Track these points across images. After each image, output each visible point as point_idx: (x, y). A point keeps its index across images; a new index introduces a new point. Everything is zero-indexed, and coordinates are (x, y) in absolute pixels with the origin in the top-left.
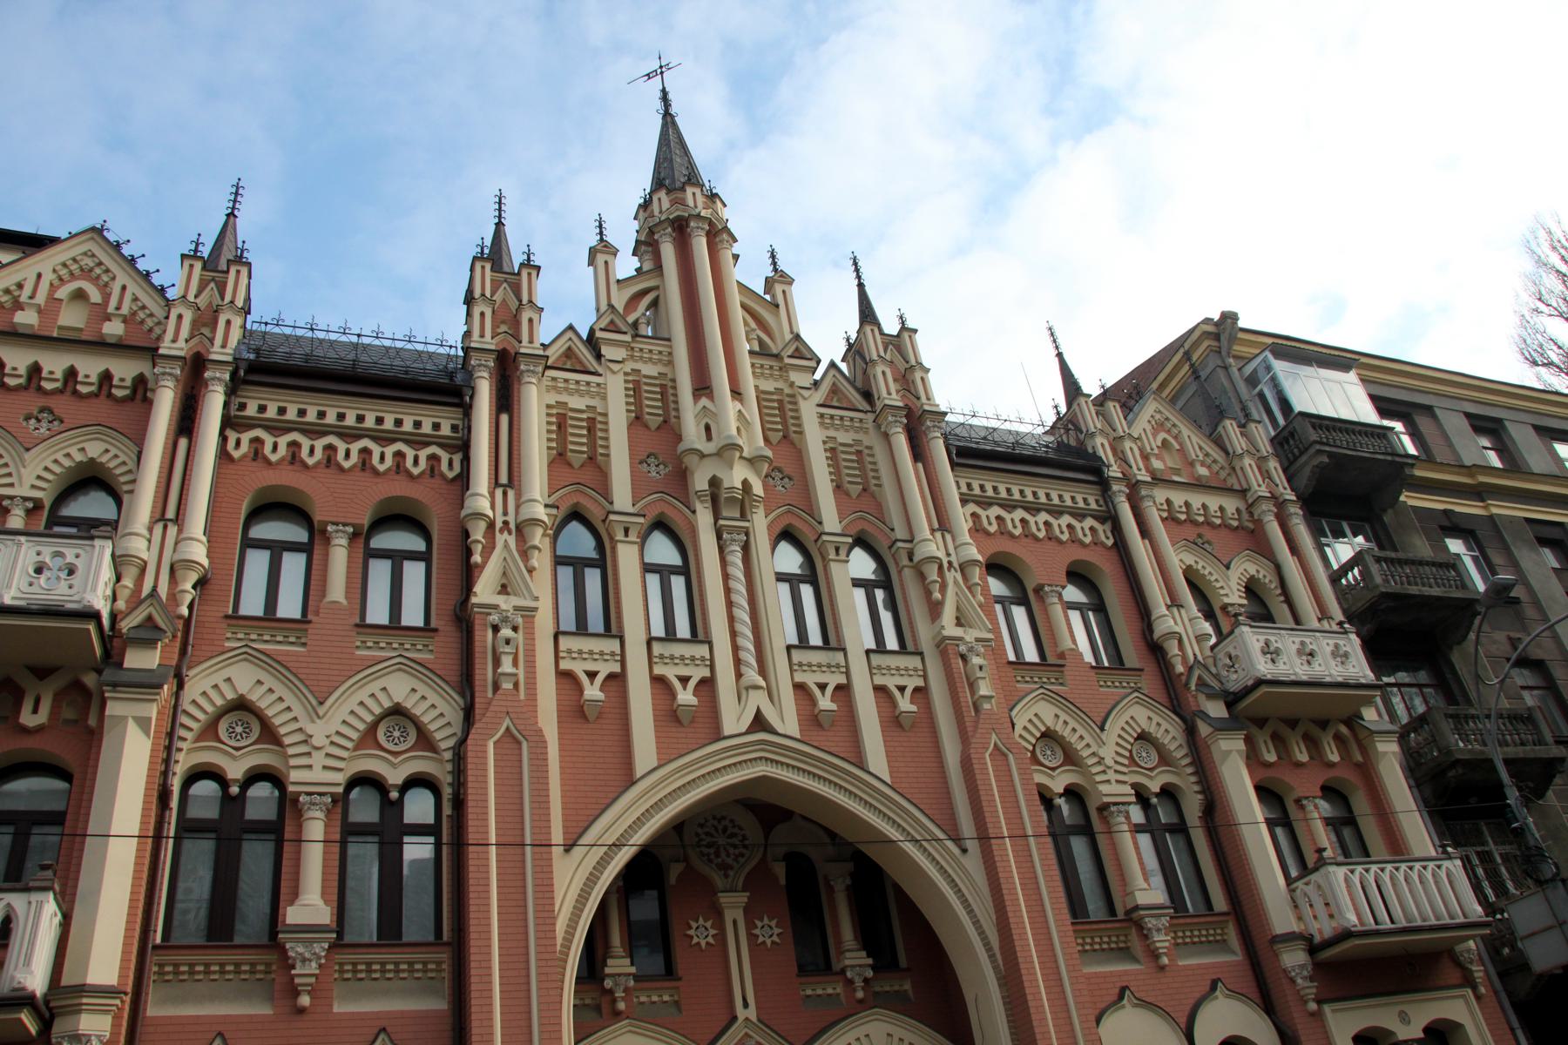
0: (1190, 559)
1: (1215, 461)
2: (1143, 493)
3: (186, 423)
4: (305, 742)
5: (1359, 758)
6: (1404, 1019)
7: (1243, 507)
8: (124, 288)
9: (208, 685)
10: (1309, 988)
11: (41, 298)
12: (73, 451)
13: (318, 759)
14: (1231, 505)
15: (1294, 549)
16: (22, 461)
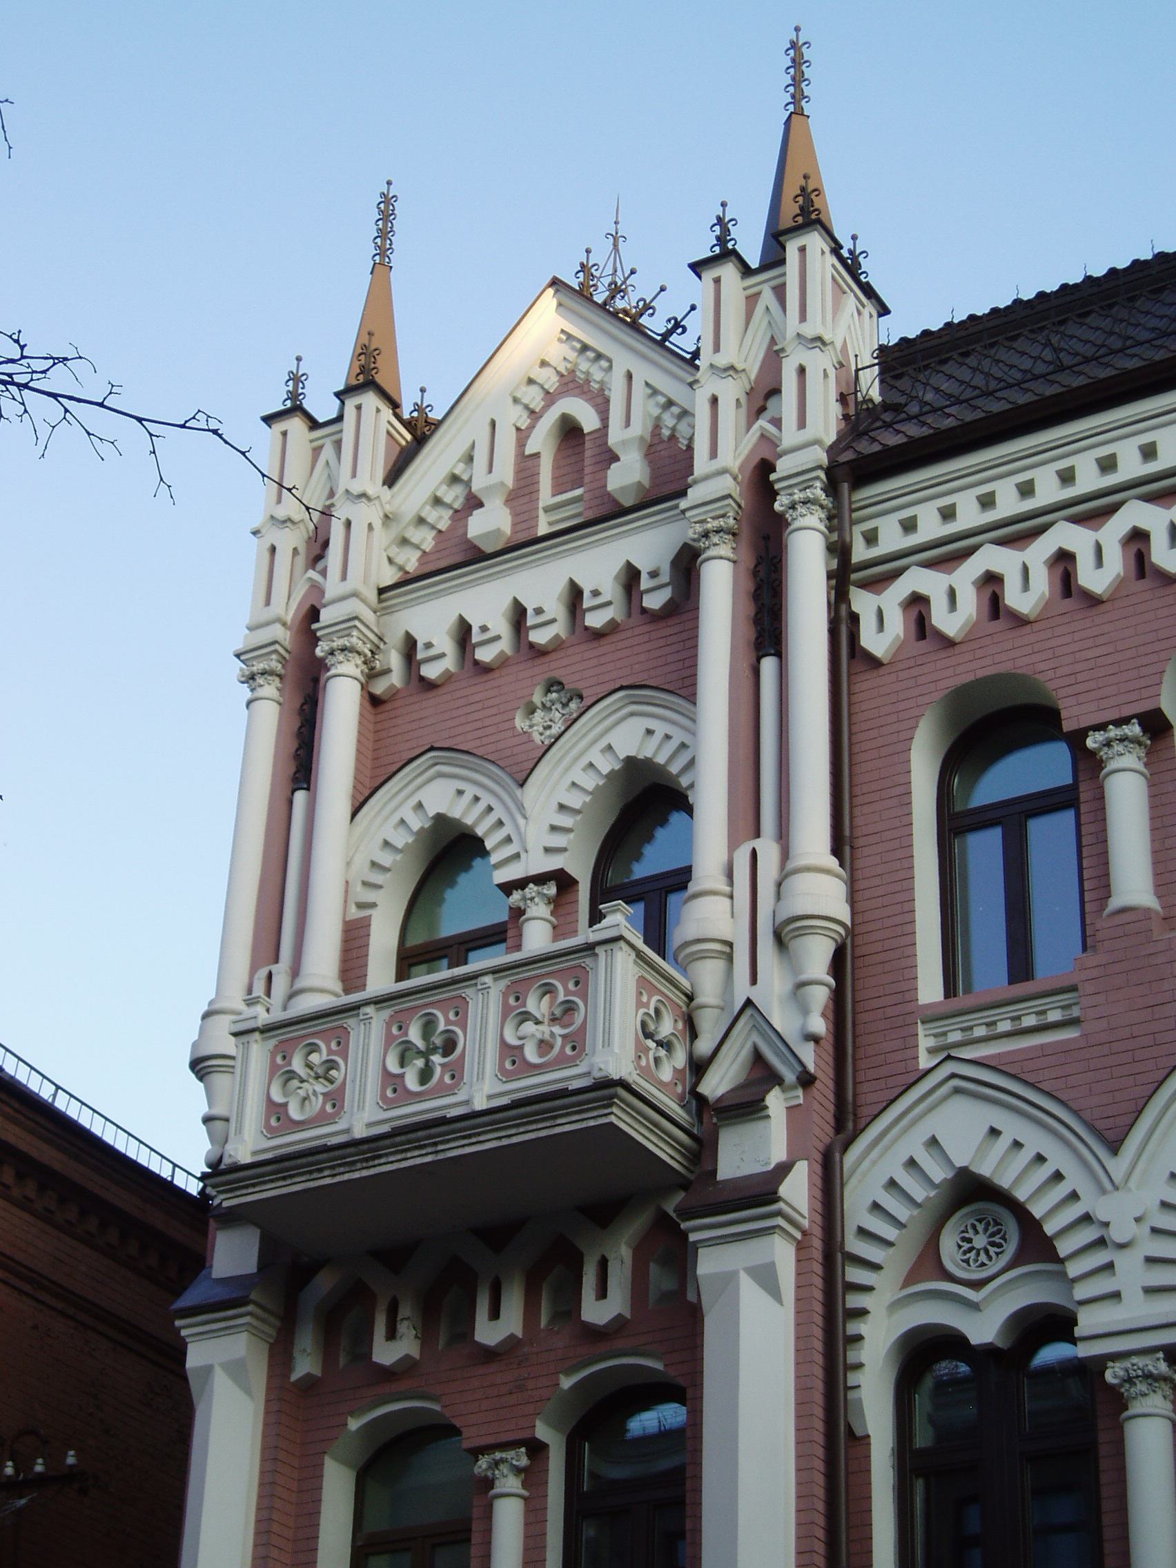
3: (766, 629)
4: (1101, 1242)
8: (629, 376)
9: (893, 1166)
11: (505, 472)
12: (595, 756)
13: (1131, 1273)
16: (521, 807)
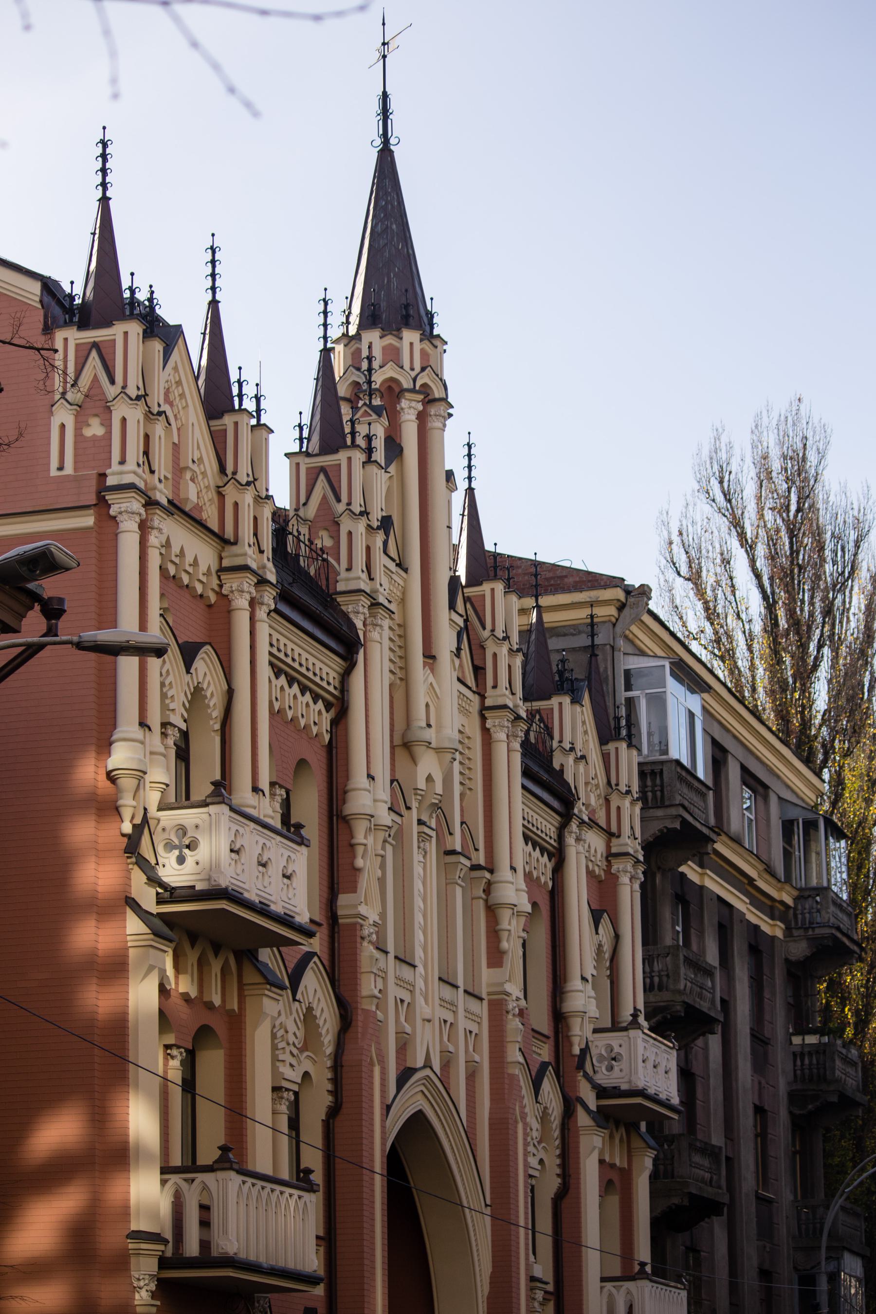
1: (204, 474)
5: (236, 1008)
7: (214, 570)
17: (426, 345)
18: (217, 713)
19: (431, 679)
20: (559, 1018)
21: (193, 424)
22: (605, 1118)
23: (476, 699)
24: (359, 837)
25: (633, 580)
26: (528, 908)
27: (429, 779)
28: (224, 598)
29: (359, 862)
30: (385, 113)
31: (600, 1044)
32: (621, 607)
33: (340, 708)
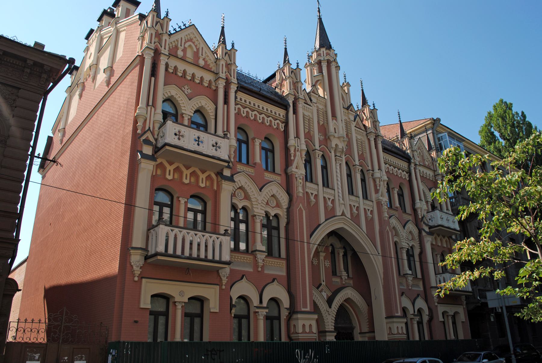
0: (173, 91)
1: (210, 59)
2: (161, 58)
5: (215, 188)
6: (182, 294)
7: (213, 81)
10: (137, 271)
14: (208, 77)
15: (226, 101)
17: (328, 51)
18: (214, 114)
19: (334, 121)
20: (415, 210)
21: (202, 48)
22: (430, 234)
23: (365, 133)
24: (292, 151)
25: (435, 118)
26: (387, 179)
27: (336, 145)
28: (217, 87)
29: (292, 158)
30: (319, 11)
31: (429, 216)
32: (434, 124)
33: (286, 123)
